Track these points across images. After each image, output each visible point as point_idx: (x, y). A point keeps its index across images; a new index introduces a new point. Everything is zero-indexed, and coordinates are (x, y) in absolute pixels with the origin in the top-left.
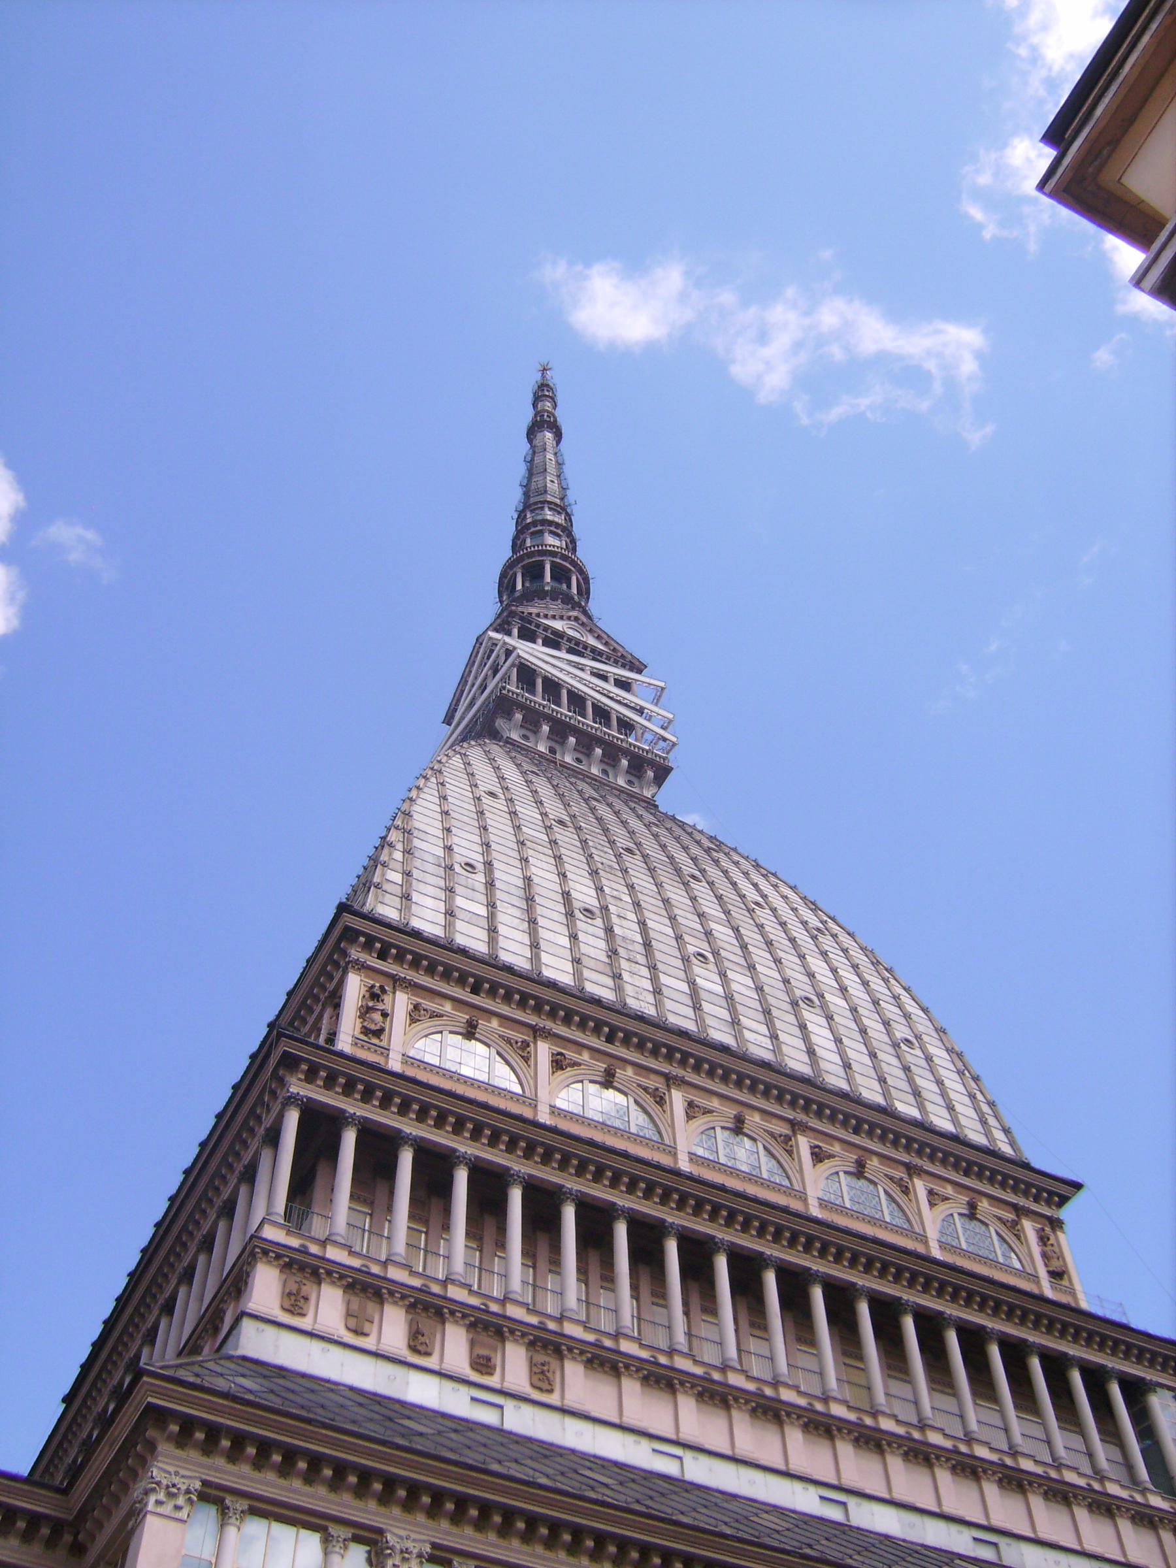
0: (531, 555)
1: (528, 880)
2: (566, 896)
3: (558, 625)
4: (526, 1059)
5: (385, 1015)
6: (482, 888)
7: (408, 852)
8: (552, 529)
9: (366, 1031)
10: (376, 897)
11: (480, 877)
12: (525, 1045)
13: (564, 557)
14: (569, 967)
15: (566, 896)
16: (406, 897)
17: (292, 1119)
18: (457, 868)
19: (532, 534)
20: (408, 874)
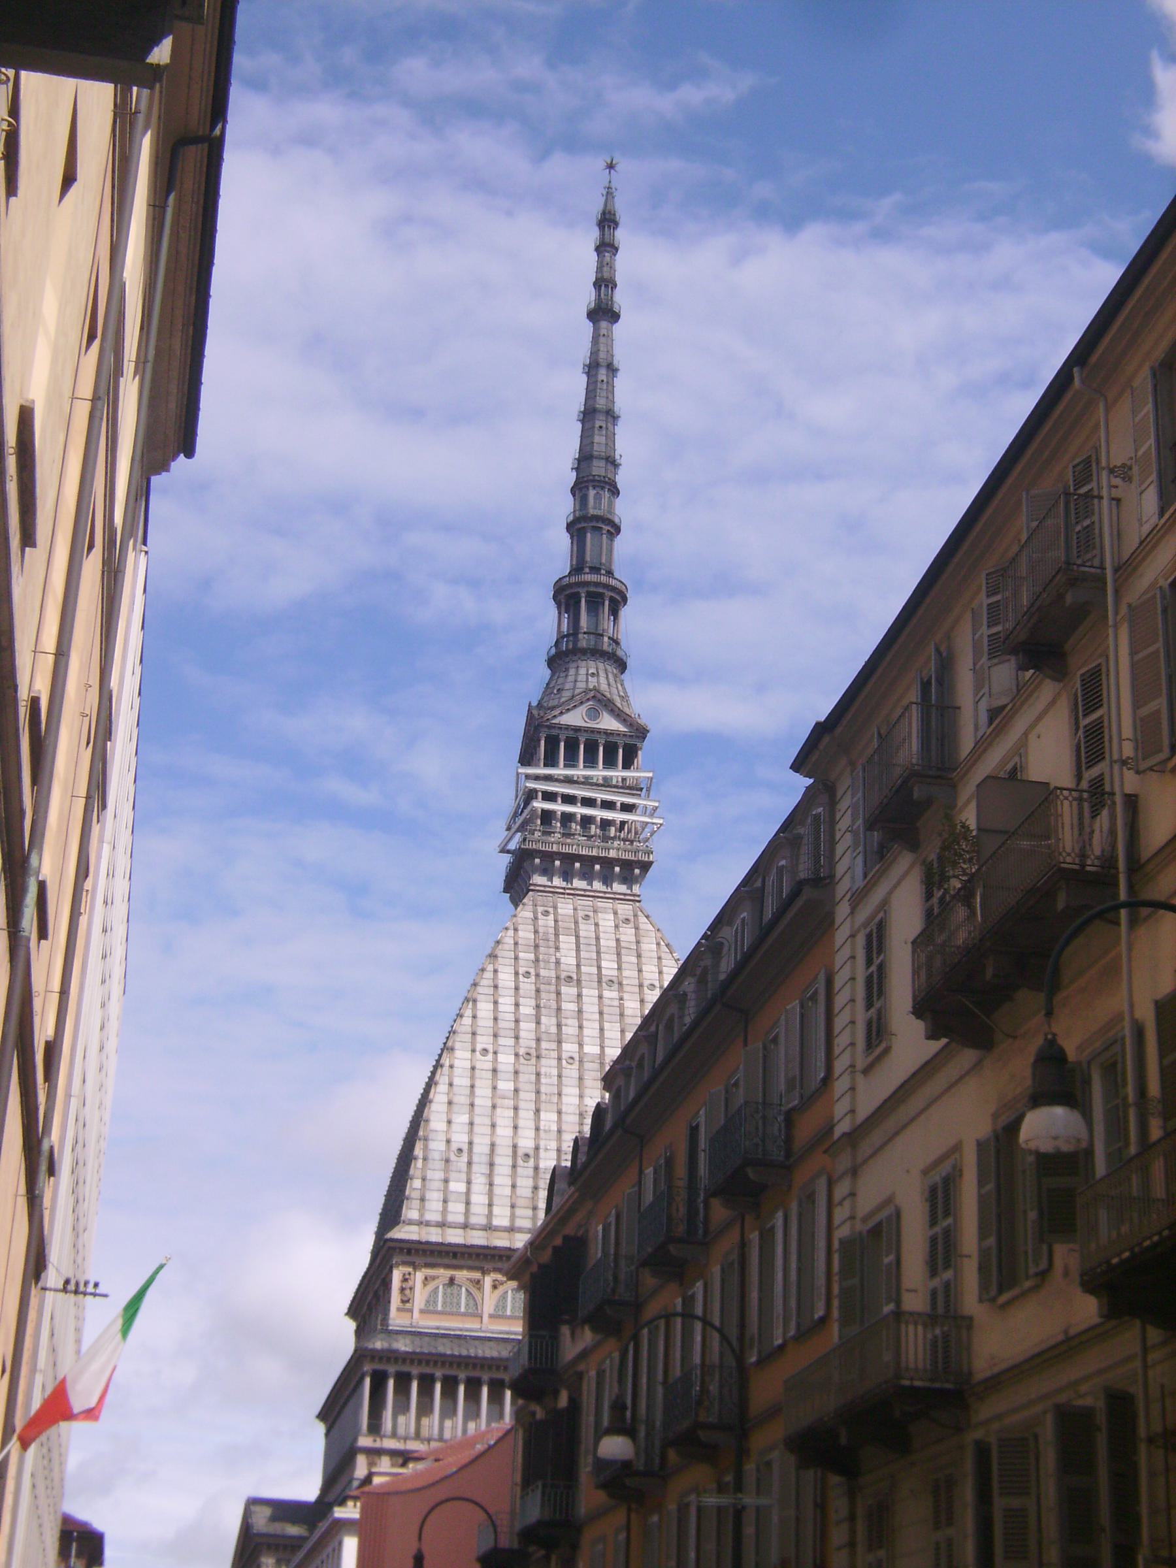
0: (570, 586)
1: (493, 1145)
2: (515, 1147)
3: (575, 718)
4: (479, 1289)
5: (411, 1289)
6: (464, 1167)
7: (425, 1159)
8: (594, 524)
9: (403, 1302)
10: (407, 1206)
11: (465, 1158)
12: (478, 1282)
13: (597, 584)
14: (508, 1211)
15: (515, 1147)
16: (423, 1199)
17: (367, 1381)
18: (453, 1157)
19: (579, 530)
20: (424, 1179)
